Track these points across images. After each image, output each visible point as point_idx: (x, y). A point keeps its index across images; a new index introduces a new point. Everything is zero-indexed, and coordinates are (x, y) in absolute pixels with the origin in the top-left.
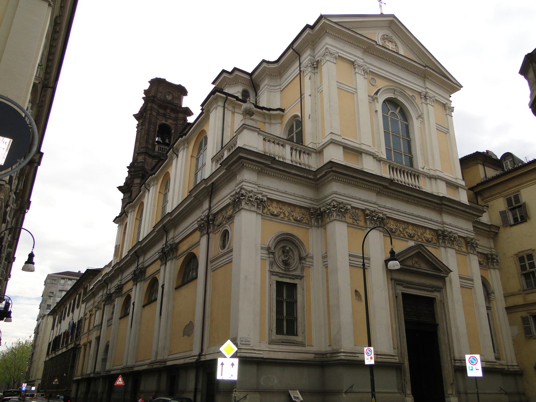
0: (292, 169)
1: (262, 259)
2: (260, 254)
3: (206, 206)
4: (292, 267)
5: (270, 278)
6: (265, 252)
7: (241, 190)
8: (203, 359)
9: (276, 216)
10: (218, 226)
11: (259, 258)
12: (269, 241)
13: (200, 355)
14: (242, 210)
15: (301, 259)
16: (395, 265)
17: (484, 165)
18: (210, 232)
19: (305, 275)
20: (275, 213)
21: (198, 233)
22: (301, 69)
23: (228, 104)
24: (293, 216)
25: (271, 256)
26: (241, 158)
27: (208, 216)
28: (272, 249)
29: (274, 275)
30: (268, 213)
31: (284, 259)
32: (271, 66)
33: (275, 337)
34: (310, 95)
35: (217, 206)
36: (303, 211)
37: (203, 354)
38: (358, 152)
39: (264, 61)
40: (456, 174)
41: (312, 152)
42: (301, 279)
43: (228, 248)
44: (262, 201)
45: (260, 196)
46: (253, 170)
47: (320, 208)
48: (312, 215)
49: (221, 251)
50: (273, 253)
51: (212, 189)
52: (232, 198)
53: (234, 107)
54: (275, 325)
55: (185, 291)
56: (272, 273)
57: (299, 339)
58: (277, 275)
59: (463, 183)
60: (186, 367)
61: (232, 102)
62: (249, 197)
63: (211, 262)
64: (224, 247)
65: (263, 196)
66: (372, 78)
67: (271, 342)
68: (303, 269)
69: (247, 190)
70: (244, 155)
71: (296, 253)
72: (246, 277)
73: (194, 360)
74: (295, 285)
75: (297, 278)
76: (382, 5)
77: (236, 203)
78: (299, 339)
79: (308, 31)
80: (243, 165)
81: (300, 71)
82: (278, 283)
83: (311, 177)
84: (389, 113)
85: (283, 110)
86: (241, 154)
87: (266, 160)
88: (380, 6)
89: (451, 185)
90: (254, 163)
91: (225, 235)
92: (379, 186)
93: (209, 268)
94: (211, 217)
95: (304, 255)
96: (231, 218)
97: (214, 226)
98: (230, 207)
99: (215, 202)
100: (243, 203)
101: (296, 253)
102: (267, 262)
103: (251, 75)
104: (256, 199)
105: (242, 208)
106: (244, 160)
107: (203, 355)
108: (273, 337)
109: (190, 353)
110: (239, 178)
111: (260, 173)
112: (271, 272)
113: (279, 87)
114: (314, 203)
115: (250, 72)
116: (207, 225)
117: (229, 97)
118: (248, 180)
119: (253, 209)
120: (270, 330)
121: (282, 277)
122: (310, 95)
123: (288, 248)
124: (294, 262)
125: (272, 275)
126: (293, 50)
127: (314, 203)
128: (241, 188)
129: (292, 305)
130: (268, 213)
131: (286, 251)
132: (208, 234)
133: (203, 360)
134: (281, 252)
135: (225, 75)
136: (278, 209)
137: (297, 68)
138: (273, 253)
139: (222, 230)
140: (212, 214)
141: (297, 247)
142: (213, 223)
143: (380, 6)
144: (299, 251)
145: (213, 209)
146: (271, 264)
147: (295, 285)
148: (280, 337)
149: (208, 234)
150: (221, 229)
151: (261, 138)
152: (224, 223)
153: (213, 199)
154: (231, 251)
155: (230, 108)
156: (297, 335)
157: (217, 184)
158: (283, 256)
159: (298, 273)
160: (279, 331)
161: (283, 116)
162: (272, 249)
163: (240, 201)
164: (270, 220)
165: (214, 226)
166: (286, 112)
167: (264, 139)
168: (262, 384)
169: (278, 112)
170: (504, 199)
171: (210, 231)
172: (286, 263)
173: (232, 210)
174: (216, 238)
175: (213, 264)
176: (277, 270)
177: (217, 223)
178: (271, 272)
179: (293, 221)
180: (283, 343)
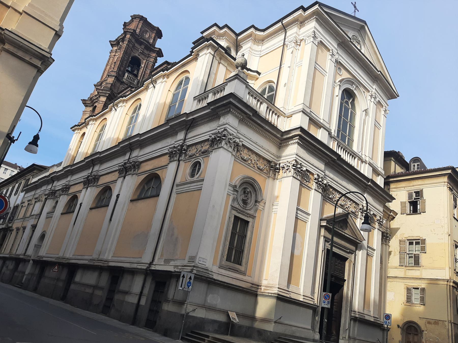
0: (266, 125)
1: (227, 194)
2: (227, 189)
3: (181, 136)
4: (249, 207)
5: (230, 212)
6: (232, 189)
7: (223, 131)
8: (153, 268)
9: (245, 160)
10: (190, 156)
11: (226, 192)
12: (237, 181)
13: (151, 264)
14: (222, 149)
15: (256, 201)
16: (324, 223)
17: (396, 163)
18: (181, 160)
19: (257, 215)
20: (245, 158)
21: (167, 157)
22: (286, 43)
23: (217, 55)
24: (257, 164)
25: (236, 193)
26: (230, 103)
27: (182, 146)
28: (238, 187)
29: (234, 210)
30: (240, 156)
31: (244, 198)
32: (258, 33)
33: (224, 262)
34: (289, 67)
35: (192, 139)
36: (266, 163)
37: (154, 263)
38: (318, 125)
39: (253, 26)
40: (379, 163)
41: (282, 115)
42: (253, 218)
43: (198, 178)
44: (238, 145)
45: (238, 140)
46: (236, 117)
47: (280, 164)
48: (272, 168)
49: (190, 178)
50: (237, 191)
51: (192, 123)
52: (213, 136)
53: (221, 59)
54: (226, 252)
55: (142, 204)
56: (233, 208)
57: (242, 268)
58: (236, 211)
59: (383, 172)
60: (133, 272)
61: (221, 54)
62: (229, 139)
63: (177, 186)
64: (192, 175)
65: (240, 141)
66: (339, 68)
67: (221, 267)
68: (256, 210)
69: (229, 133)
70: (234, 102)
71: (253, 196)
72: (214, 206)
73: (145, 268)
74: (248, 222)
75: (250, 217)
76: (356, 11)
77: (215, 142)
78: (242, 268)
79: (300, 12)
80: (230, 110)
81: (284, 44)
82: (235, 217)
83: (279, 136)
84: (345, 100)
85: (259, 74)
86: (231, 100)
87: (250, 111)
88: (355, 11)
89: (375, 171)
90: (239, 111)
91: (196, 166)
92: (329, 159)
93: (174, 190)
94: (185, 147)
95: (259, 200)
96: (206, 153)
97: (186, 155)
98: (206, 143)
99: (190, 135)
100: (223, 142)
101: (253, 196)
102: (231, 198)
103: (237, 35)
104: (234, 142)
105: (222, 147)
106: (232, 106)
107: (153, 264)
108: (223, 263)
109: (139, 260)
110: (223, 120)
111: (241, 121)
112: (232, 206)
113: (259, 53)
114: (275, 158)
115: (238, 32)
116: (177, 153)
117: (220, 48)
118: (230, 122)
119: (230, 149)
120: (222, 256)
121: (240, 213)
122: (289, 67)
123: (249, 190)
124: (251, 202)
125: (233, 209)
126: (282, 24)
127: (275, 158)
128: (225, 130)
129: (243, 237)
130: (240, 156)
131: (247, 192)
132: (179, 161)
133: (153, 268)
134: (243, 192)
135: (215, 28)
136: (248, 156)
137: (281, 41)
138: (237, 191)
139: (193, 161)
140: (186, 145)
141: (255, 191)
142: (185, 153)
143: (355, 11)
144: (256, 195)
145: (187, 141)
146: (234, 200)
147: (248, 222)
148: (228, 263)
149: (179, 161)
150: (193, 159)
151: (248, 91)
152: (198, 155)
153: (190, 132)
154: (203, 180)
155: (218, 58)
156: (240, 265)
157: (197, 120)
158: (243, 196)
159: (251, 212)
160: (228, 259)
161: (257, 79)
162: (238, 187)
163: (220, 140)
164: (240, 163)
165: (186, 155)
166: (261, 76)
167: (249, 93)
168: (209, 301)
169: (255, 74)
170: (407, 193)
171: (180, 159)
172: (245, 202)
173: (208, 146)
174: (186, 168)
175: (179, 187)
176: (237, 206)
177: (190, 153)
178: (232, 206)
179: (256, 168)
180: (230, 269)
